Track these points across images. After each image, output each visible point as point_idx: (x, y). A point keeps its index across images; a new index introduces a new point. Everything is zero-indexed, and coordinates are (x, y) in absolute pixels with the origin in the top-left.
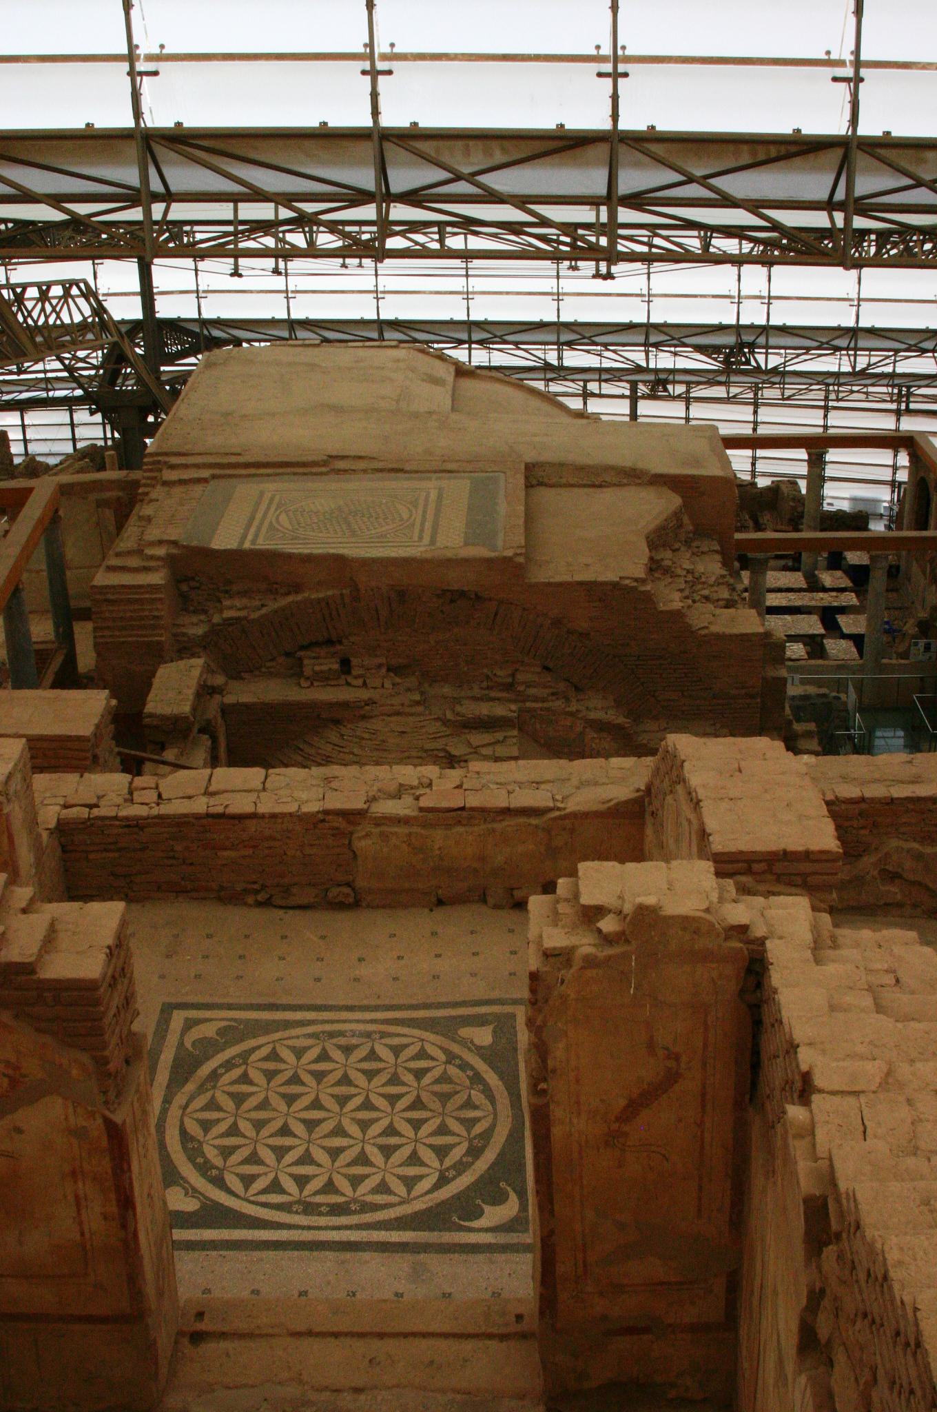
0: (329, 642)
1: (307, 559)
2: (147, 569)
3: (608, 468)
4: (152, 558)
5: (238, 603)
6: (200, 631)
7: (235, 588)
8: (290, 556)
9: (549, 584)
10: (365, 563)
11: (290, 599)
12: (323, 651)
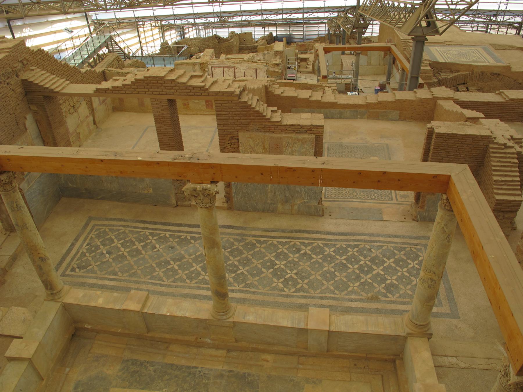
0: (464, 84)
1: (462, 65)
2: (426, 66)
3: (507, 45)
4: (426, 63)
6: (436, 80)
7: (443, 71)
8: (458, 64)
9: (516, 72)
10: (477, 66)
11: (456, 74)
12: (462, 86)
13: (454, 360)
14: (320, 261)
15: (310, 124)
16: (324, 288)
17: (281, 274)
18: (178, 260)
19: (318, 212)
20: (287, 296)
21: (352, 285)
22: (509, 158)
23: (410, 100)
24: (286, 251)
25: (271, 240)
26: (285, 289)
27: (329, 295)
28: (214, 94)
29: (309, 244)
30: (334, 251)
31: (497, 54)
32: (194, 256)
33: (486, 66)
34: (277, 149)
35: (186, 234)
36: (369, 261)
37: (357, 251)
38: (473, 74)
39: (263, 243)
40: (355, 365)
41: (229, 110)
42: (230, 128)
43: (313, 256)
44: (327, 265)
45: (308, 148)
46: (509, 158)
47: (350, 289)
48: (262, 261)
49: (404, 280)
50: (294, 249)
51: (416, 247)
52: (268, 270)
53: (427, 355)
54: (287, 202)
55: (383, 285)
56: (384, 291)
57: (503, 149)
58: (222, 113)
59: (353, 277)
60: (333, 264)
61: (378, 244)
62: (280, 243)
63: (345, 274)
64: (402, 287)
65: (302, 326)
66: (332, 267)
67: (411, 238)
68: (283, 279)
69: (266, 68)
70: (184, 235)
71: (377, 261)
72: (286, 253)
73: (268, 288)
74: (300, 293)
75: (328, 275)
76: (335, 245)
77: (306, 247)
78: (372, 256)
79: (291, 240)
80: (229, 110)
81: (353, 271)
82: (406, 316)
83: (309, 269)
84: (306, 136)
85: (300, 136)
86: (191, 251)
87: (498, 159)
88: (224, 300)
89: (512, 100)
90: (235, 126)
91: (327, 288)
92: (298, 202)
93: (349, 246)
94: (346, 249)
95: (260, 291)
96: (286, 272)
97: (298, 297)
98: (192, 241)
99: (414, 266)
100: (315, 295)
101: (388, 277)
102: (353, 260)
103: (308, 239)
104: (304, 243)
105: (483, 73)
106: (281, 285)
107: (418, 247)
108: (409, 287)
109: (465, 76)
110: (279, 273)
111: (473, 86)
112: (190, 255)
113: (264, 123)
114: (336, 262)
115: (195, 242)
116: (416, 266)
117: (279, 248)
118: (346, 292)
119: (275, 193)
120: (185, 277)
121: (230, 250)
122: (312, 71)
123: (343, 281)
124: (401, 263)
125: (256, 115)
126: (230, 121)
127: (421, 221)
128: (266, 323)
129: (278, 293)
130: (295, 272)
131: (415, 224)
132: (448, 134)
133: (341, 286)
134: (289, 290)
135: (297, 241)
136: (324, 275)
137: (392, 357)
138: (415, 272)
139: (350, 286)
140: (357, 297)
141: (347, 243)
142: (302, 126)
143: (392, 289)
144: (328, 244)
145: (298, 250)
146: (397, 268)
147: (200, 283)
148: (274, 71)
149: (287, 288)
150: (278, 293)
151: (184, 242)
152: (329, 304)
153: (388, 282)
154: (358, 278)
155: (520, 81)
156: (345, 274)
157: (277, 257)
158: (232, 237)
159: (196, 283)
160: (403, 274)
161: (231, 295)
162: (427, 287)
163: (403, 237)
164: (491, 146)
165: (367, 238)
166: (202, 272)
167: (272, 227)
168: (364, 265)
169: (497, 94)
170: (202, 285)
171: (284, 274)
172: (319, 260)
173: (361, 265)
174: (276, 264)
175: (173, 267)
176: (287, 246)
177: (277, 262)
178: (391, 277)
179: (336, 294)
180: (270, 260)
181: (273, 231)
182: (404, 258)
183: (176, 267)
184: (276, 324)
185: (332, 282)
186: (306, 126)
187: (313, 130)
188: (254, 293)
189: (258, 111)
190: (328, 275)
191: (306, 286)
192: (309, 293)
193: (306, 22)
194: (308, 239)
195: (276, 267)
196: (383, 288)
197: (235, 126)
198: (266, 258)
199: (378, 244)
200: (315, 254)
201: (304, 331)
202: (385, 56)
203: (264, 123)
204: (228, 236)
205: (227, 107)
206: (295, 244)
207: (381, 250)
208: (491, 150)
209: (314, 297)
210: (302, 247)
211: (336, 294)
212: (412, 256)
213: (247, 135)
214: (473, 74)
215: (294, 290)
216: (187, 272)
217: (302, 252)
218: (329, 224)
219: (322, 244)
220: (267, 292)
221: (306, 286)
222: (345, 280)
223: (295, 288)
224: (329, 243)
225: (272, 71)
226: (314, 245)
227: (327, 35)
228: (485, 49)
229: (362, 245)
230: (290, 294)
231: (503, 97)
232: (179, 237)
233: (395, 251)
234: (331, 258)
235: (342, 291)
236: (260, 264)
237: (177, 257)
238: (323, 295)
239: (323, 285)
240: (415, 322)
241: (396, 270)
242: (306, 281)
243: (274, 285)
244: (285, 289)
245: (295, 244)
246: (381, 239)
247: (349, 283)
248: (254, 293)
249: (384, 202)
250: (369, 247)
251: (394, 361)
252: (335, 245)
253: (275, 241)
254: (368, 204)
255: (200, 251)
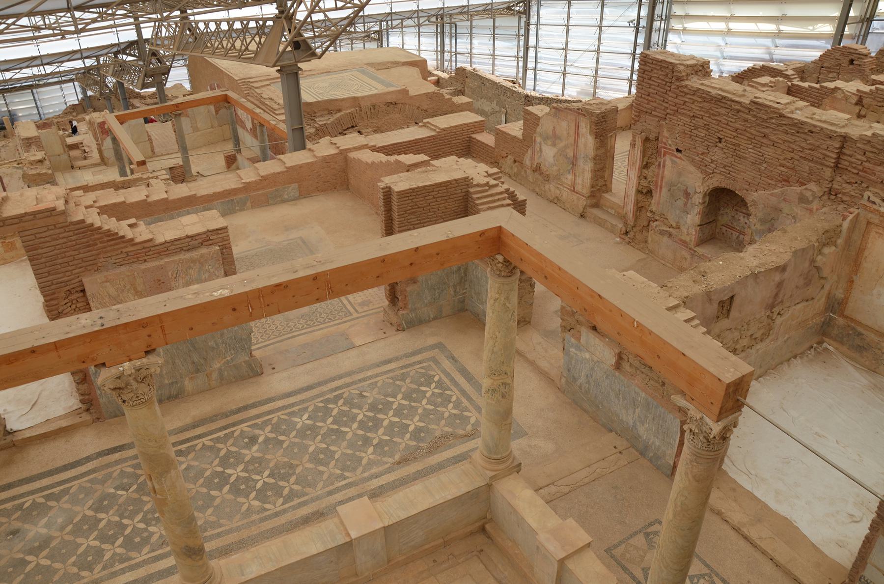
0: (353, 127)
1: (343, 100)
3: (388, 62)
5: (322, 119)
6: (313, 130)
8: (337, 100)
10: (363, 98)
11: (339, 115)
12: (351, 130)
13: (553, 489)
14: (297, 440)
15: (204, 230)
16: (325, 477)
17: (247, 487)
18: (41, 548)
19: (254, 371)
20: (277, 514)
21: (363, 455)
22: (499, 200)
23: (308, 164)
24: (233, 449)
25: (199, 443)
26: (267, 506)
27: (340, 484)
28: (17, 221)
29: (266, 423)
30: (309, 418)
31: (382, 75)
32: (70, 527)
33: (375, 95)
34: (160, 285)
35: (31, 497)
36: (369, 410)
37: (344, 404)
38: (361, 110)
39: (189, 453)
40: (435, 561)
41: (52, 243)
42: (61, 275)
43: (282, 438)
44: (310, 443)
45: (212, 270)
46: (499, 200)
47: (364, 462)
48: (202, 480)
49: (432, 416)
50: (246, 440)
51: (421, 365)
52: (221, 491)
53: (529, 493)
54: (198, 371)
55: (408, 436)
56: (415, 443)
57: (487, 191)
58: (40, 251)
59: (360, 443)
60: (319, 437)
61: (368, 382)
62: (218, 440)
63: (345, 444)
64: (434, 427)
65: (341, 540)
66: (321, 442)
67: (407, 356)
68: (254, 493)
69: (20, 171)
70: (28, 502)
71: (380, 407)
72: (236, 452)
73: (238, 516)
74: (292, 500)
75: (322, 456)
76: (305, 409)
77: (263, 429)
78: (369, 402)
79: (233, 429)
80: (52, 243)
81: (355, 434)
82: (477, 456)
83: (286, 460)
84: (204, 251)
85: (194, 254)
86: (60, 520)
87: (487, 206)
88: (201, 559)
89: (444, 130)
90: (70, 268)
91: (331, 475)
92: (217, 365)
93: (327, 401)
94: (326, 407)
95: (227, 528)
96: (253, 480)
97: (294, 508)
98: (52, 503)
99: (433, 393)
100: (319, 492)
101: (408, 422)
102: (345, 419)
103: (258, 416)
104: (256, 424)
105: (374, 106)
106: (256, 503)
107: (425, 364)
108: (443, 422)
109: (352, 116)
110: (243, 487)
111: (366, 127)
112: (62, 528)
113: (124, 250)
114: (322, 432)
115: (58, 502)
116: (436, 391)
117: (219, 450)
118: (361, 468)
119: (174, 363)
120: (75, 570)
121: (135, 487)
122: (99, 161)
123: (348, 455)
124: (414, 396)
125: (106, 239)
126: (60, 261)
127: (408, 328)
128: (284, 564)
129: (258, 516)
130: (267, 473)
131: (401, 335)
132: (413, 189)
133: (349, 463)
134: (274, 504)
135: (243, 426)
136: (314, 459)
137: (478, 524)
138: (439, 400)
139: (362, 458)
140: (381, 469)
141: (322, 399)
142: (192, 237)
143: (422, 435)
144: (294, 412)
145: (253, 440)
146: (413, 404)
147: (112, 566)
148: (39, 174)
149: (270, 503)
150: (258, 516)
151: (35, 513)
152: (346, 497)
153: (411, 428)
154: (367, 441)
155: (425, 107)
156: (345, 444)
157: (224, 462)
158: (127, 464)
159: (104, 569)
160: (425, 409)
161: (208, 547)
162: (500, 398)
163: (397, 359)
164: (472, 190)
165: (348, 380)
166: (103, 546)
167: (189, 420)
168: (365, 419)
169: (421, 126)
170: (118, 567)
171: (251, 483)
172: (293, 440)
173: (361, 422)
174: (230, 475)
175: (38, 564)
176: (231, 441)
177: (229, 471)
178: (412, 420)
179: (348, 478)
180: (216, 474)
181: (194, 426)
182: (414, 386)
183: (45, 562)
184: (298, 558)
185: (333, 463)
186: (198, 235)
187: (212, 238)
188: (219, 535)
189: (109, 230)
190: (322, 456)
191: (296, 487)
192: (307, 494)
193: (32, 86)
194: (258, 416)
195: (232, 479)
196: (410, 439)
197: (70, 268)
198: (208, 473)
199: (370, 381)
200: (283, 434)
201: (348, 547)
202: (217, 112)
203: (124, 250)
204: (119, 466)
205: (48, 239)
206: (242, 431)
207: (376, 390)
208: (475, 196)
209: (318, 498)
210: (257, 432)
211: (348, 478)
212: (422, 380)
213: (99, 277)
214: (361, 110)
215: (281, 500)
216: (73, 559)
217: (261, 440)
218: (278, 383)
219: (285, 414)
220: (240, 523)
221: (296, 487)
222: (349, 452)
223: (281, 496)
224: (296, 408)
225: (33, 175)
226: (273, 422)
227: (83, 99)
228: (363, 72)
229: (346, 392)
230: (278, 509)
231: (432, 129)
232: (20, 507)
233: (398, 383)
234: (310, 429)
235: (355, 469)
236: (201, 486)
237: (37, 544)
238: (331, 488)
239: (321, 473)
240: (496, 457)
241: (413, 407)
242: (293, 479)
243: (245, 507)
244: (267, 506)
245: (242, 431)
246: (369, 373)
247: (357, 453)
248: (219, 535)
249: (340, 321)
250: (357, 392)
251: (483, 529)
252: (305, 409)
253: (206, 441)
254: (320, 332)
255: (78, 513)
